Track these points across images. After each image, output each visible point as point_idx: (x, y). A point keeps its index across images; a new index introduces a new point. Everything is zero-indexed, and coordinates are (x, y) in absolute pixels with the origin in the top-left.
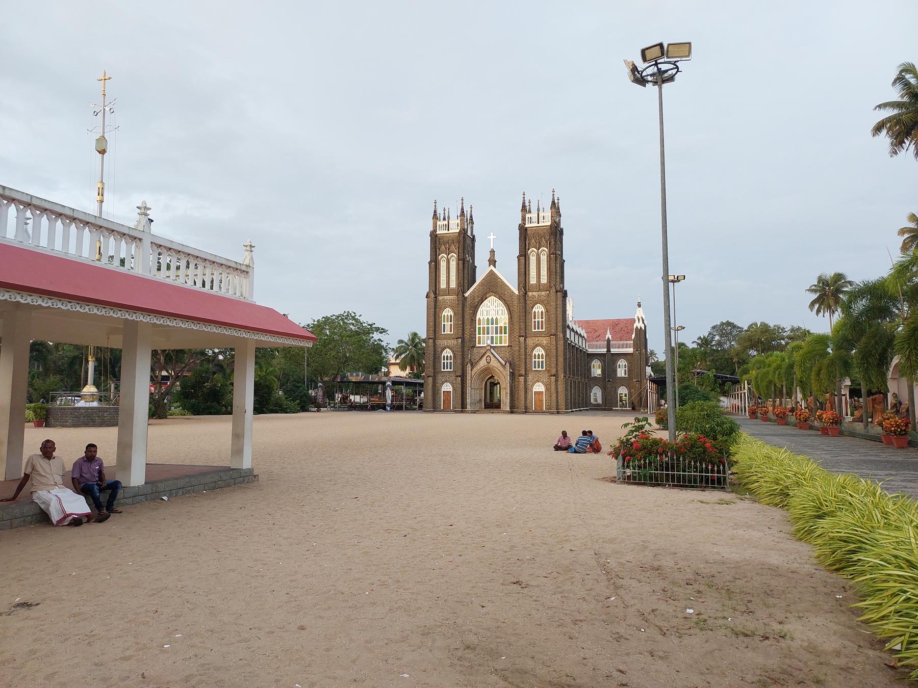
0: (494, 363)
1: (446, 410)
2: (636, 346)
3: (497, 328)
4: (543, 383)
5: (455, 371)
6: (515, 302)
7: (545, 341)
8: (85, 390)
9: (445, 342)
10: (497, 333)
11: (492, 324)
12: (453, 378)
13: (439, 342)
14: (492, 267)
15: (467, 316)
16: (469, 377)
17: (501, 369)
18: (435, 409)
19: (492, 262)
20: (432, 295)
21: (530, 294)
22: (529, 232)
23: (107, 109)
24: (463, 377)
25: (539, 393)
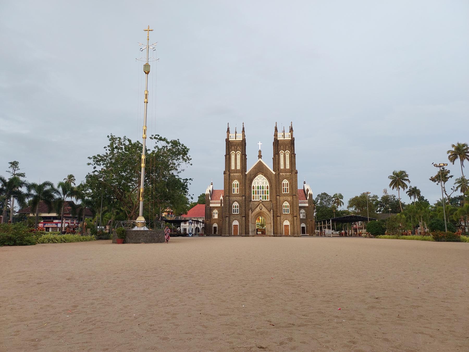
1: (236, 235)
2: (309, 203)
3: (263, 191)
4: (289, 220)
5: (240, 214)
6: (273, 178)
7: (289, 198)
8: (138, 219)
9: (235, 198)
10: (263, 194)
11: (260, 189)
12: (239, 217)
13: (231, 198)
15: (247, 185)
16: (250, 217)
17: (268, 213)
18: (230, 235)
19: (260, 156)
20: (228, 173)
21: (281, 174)
22: (279, 142)
23: (151, 47)
24: (246, 216)
25: (286, 226)
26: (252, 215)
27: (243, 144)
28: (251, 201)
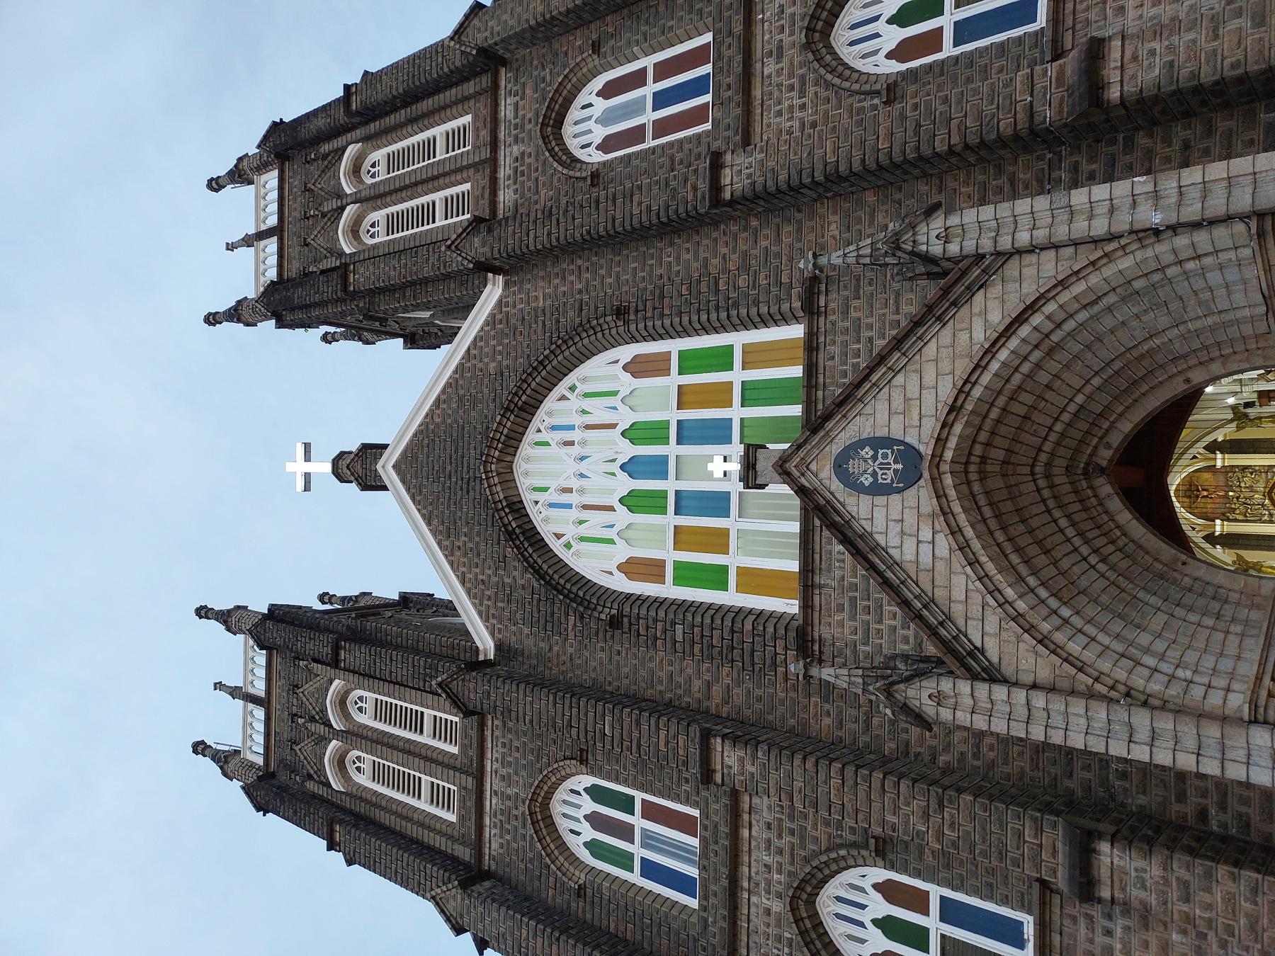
0: (913, 404)
5: (1042, 897)
14: (386, 468)
16: (1080, 728)
17: (986, 313)
21: (506, 197)
26: (1025, 659)
27: (278, 630)
28: (803, 637)
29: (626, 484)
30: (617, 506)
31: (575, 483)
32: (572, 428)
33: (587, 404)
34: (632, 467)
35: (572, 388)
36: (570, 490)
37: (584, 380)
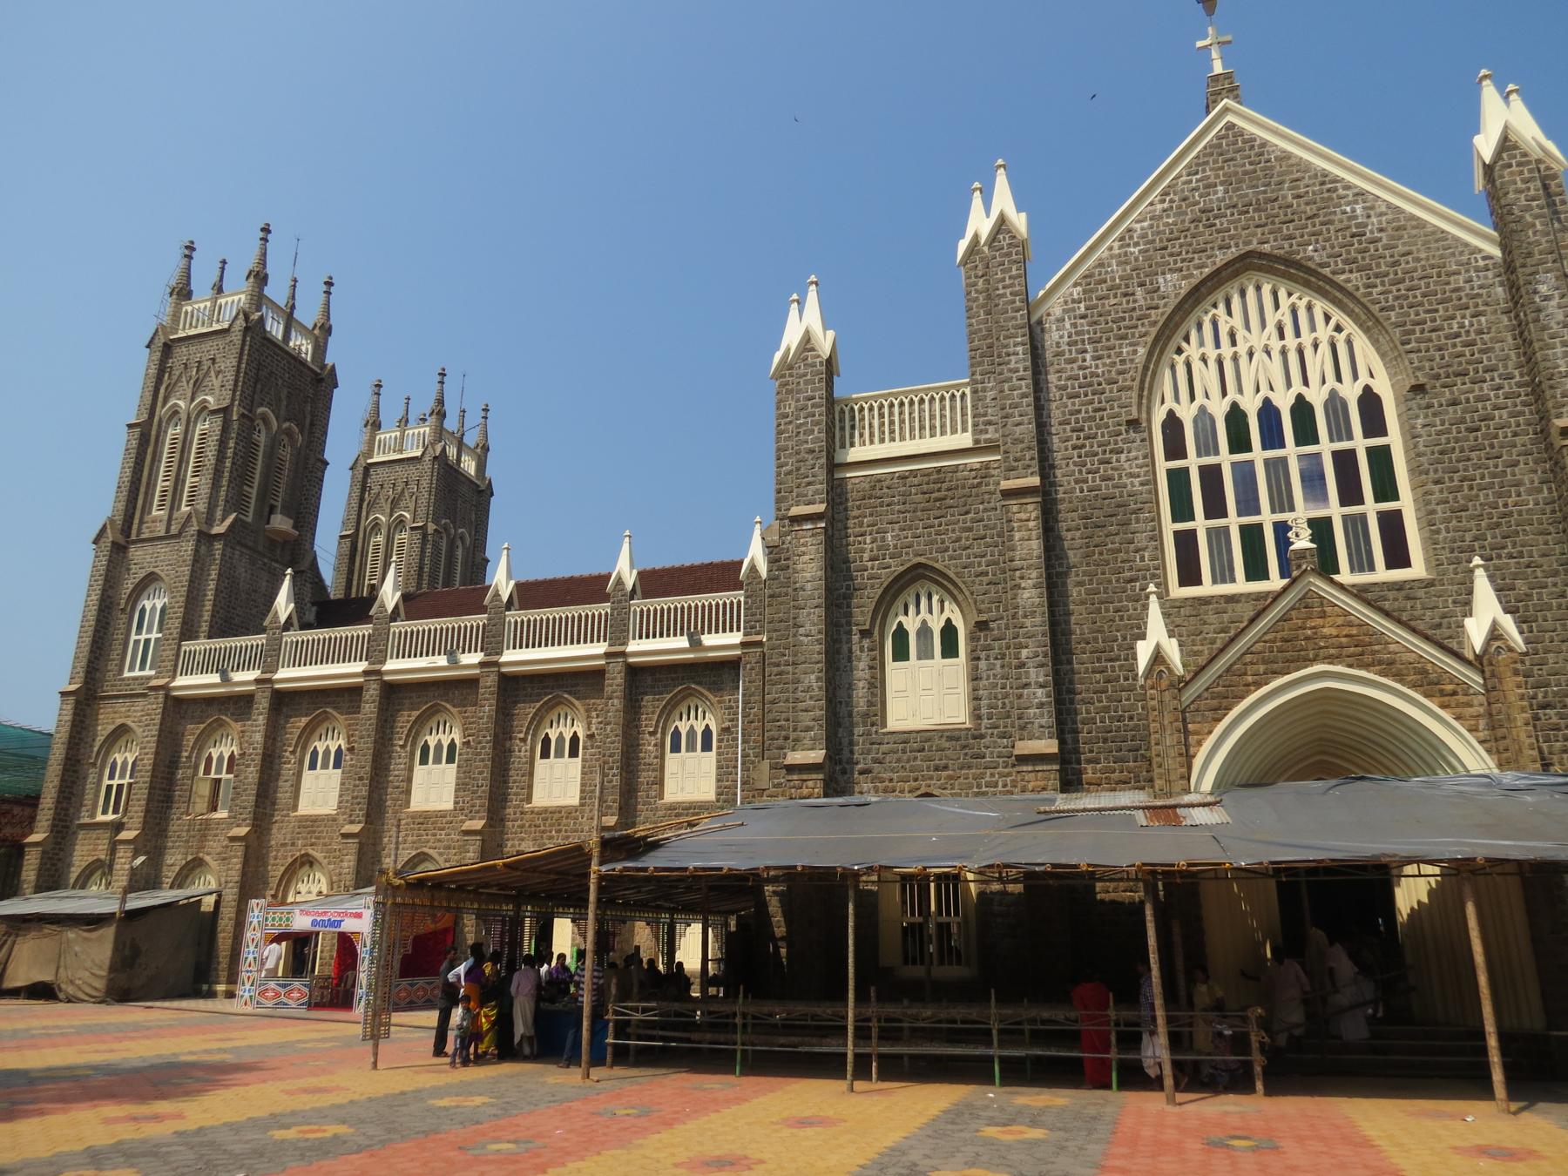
29: (1251, 405)
30: (1229, 399)
31: (1242, 349)
32: (1298, 334)
33: (1324, 348)
34: (1269, 413)
35: (1338, 329)
36: (1234, 343)
37: (1349, 342)
